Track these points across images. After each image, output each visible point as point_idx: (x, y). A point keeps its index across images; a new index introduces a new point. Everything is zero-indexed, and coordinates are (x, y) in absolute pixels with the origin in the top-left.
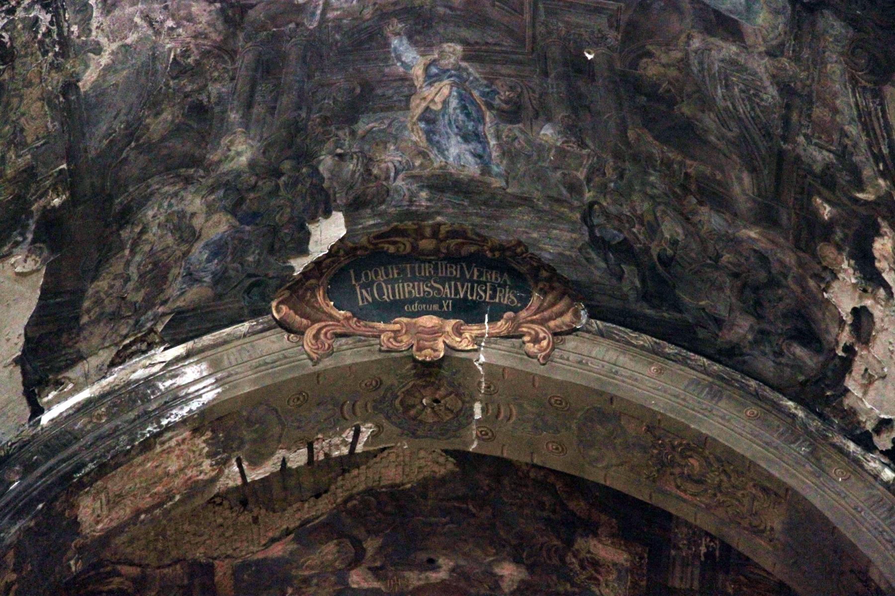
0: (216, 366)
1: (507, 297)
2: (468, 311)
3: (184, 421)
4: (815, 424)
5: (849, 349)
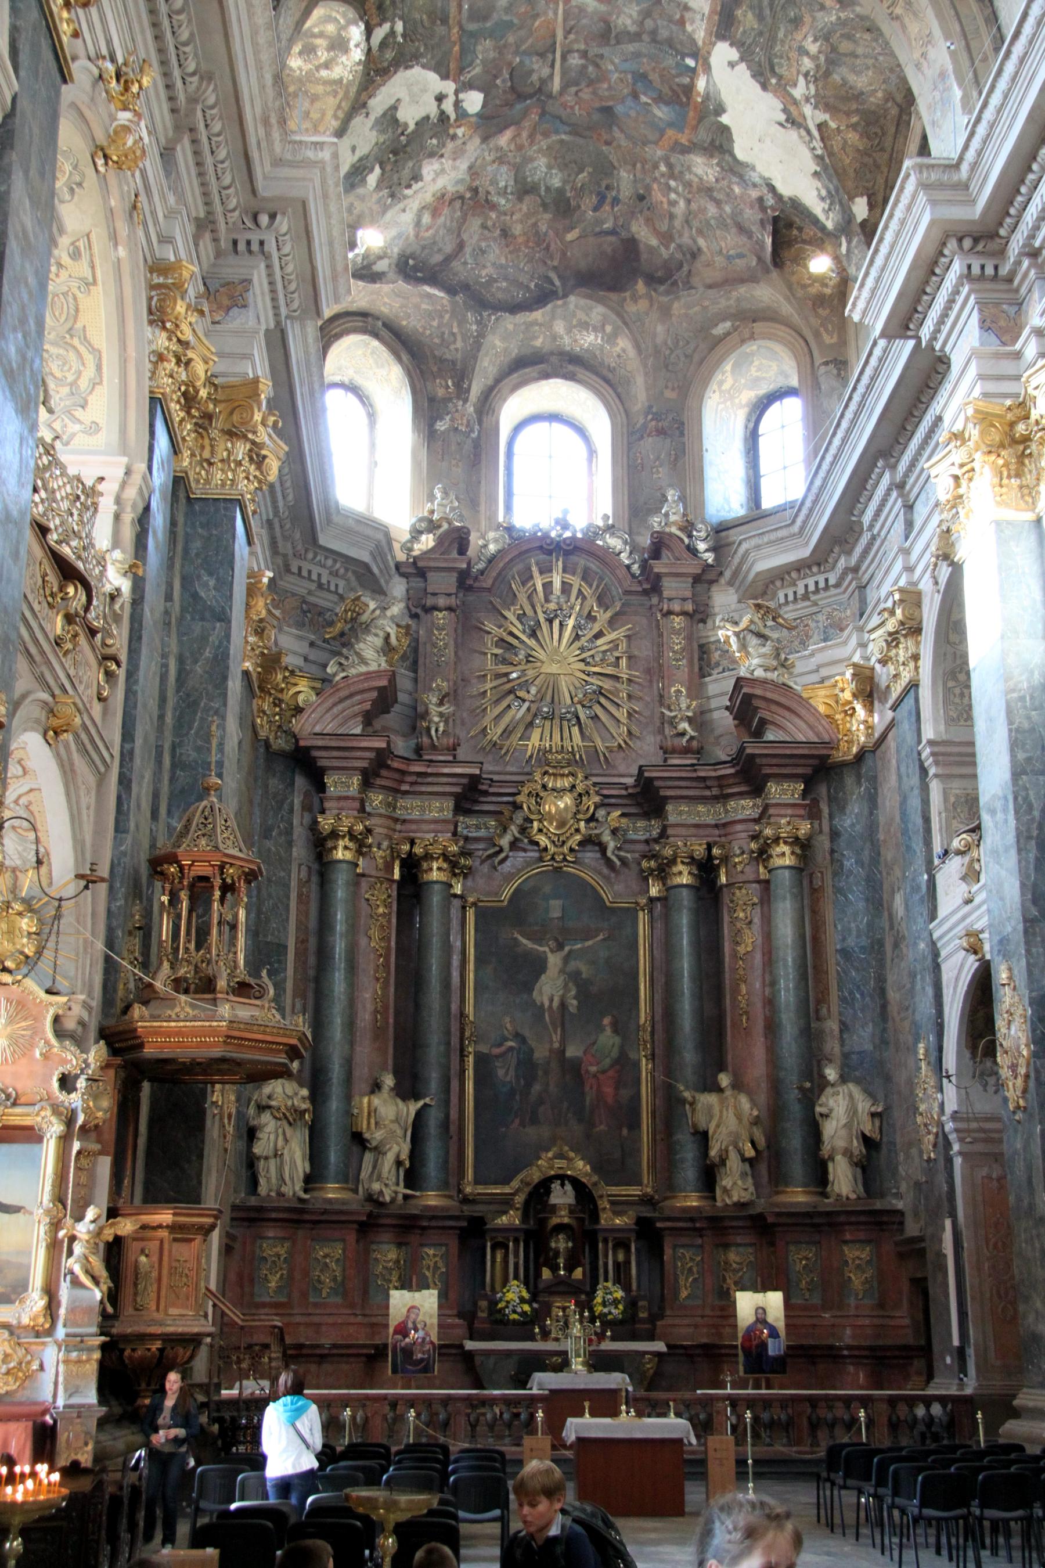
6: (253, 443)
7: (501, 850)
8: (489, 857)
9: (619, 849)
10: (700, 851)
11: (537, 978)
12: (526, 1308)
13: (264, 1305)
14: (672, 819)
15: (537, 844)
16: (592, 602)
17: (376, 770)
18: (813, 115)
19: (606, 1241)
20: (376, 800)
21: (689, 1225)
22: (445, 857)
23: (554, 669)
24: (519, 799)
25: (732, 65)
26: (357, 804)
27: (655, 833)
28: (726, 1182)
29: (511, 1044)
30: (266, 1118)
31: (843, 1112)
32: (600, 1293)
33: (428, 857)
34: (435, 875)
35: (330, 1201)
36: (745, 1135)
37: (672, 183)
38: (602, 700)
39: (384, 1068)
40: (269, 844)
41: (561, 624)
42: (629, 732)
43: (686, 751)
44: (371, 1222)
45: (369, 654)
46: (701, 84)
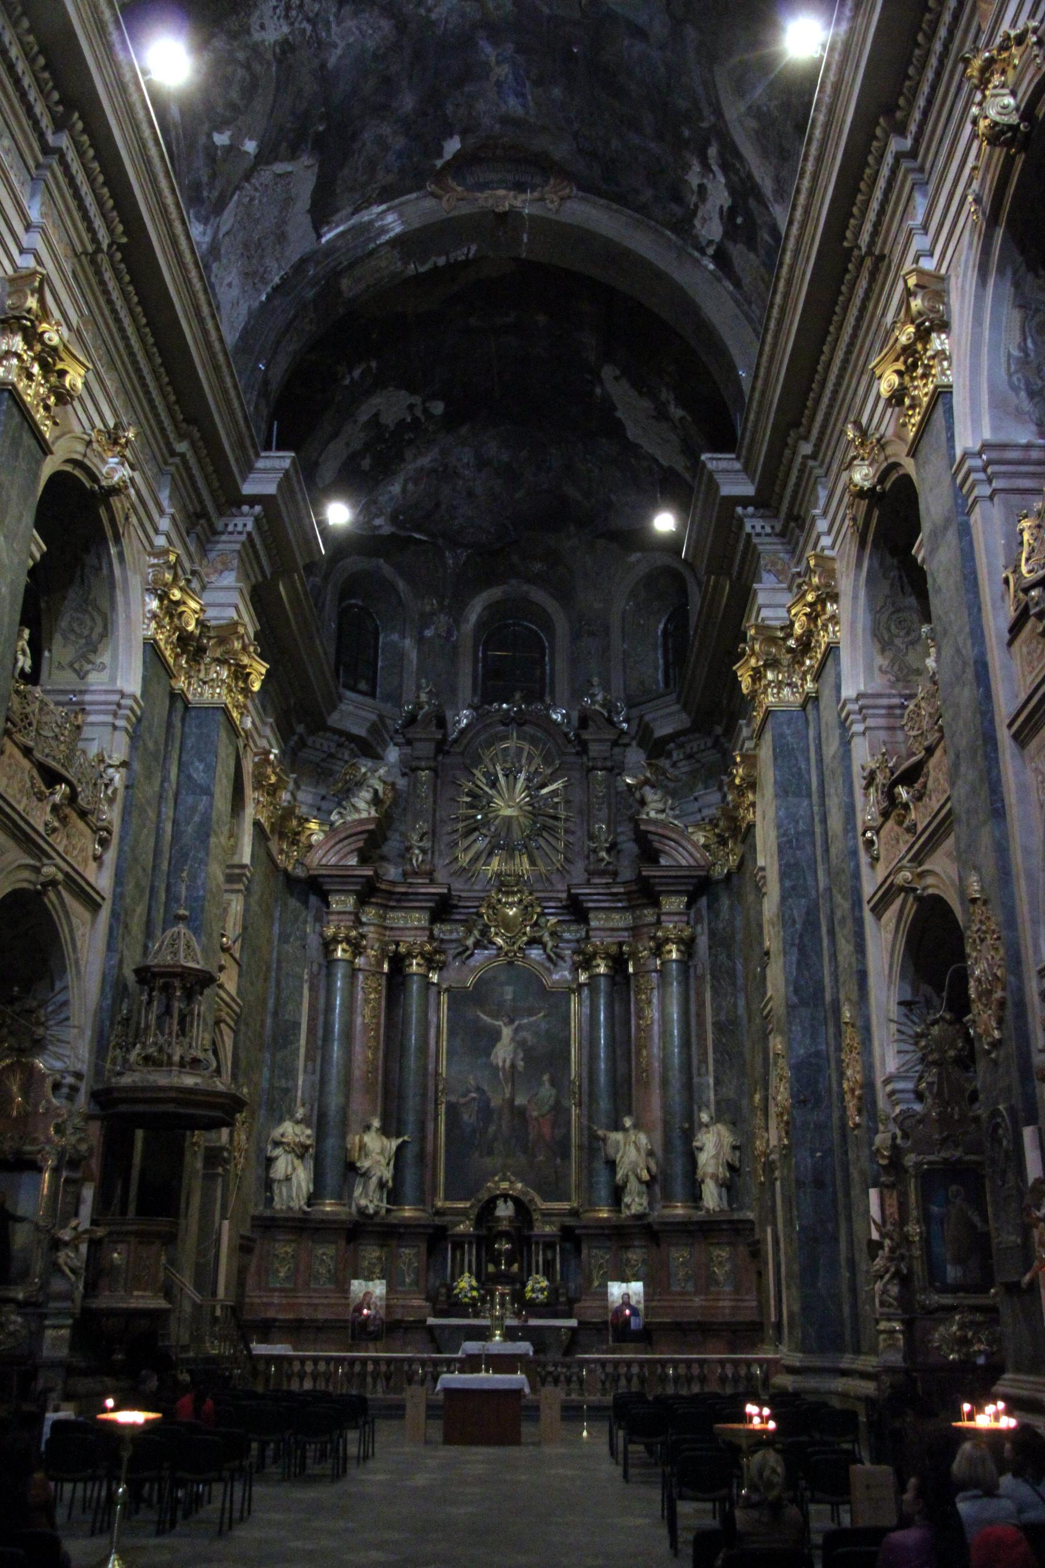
0: (401, 216)
1: (538, 180)
2: (520, 187)
3: (387, 242)
4: (680, 243)
5: (696, 206)
6: (237, 665)
7: (467, 949)
8: (460, 954)
10: (614, 949)
11: (494, 1046)
12: (475, 1293)
13: (275, 1290)
14: (593, 924)
16: (538, 760)
17: (368, 892)
18: (677, 412)
19: (537, 1244)
20: (369, 915)
21: (600, 1231)
22: (422, 954)
23: (508, 812)
25: (616, 379)
26: (352, 917)
27: (583, 934)
28: (627, 1200)
29: (473, 1095)
30: (279, 1151)
31: (713, 1145)
32: (530, 1283)
33: (409, 955)
34: (415, 968)
35: (327, 1213)
36: (642, 1165)
37: (588, 457)
38: (545, 834)
39: (373, 1114)
40: (288, 948)
43: (602, 873)
44: (358, 1230)
45: (362, 805)
46: (598, 391)
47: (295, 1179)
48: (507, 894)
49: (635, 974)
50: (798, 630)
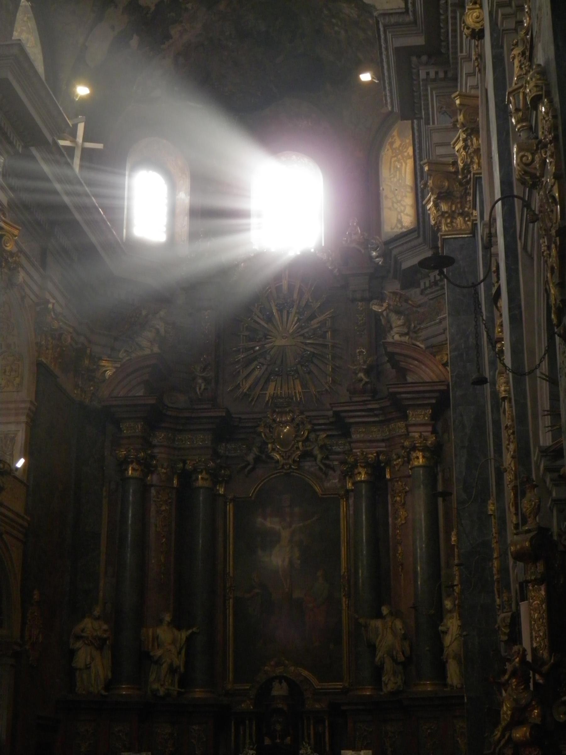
7: (249, 464)
9: (327, 458)
14: (355, 437)
15: (272, 458)
20: (159, 438)
24: (261, 429)
29: (257, 591)
30: (79, 644)
33: (195, 471)
34: (200, 483)
37: (334, 21)
38: (315, 361)
41: (288, 313)
42: (334, 381)
47: (93, 668)
48: (281, 413)
49: (391, 480)
50: (461, 165)
